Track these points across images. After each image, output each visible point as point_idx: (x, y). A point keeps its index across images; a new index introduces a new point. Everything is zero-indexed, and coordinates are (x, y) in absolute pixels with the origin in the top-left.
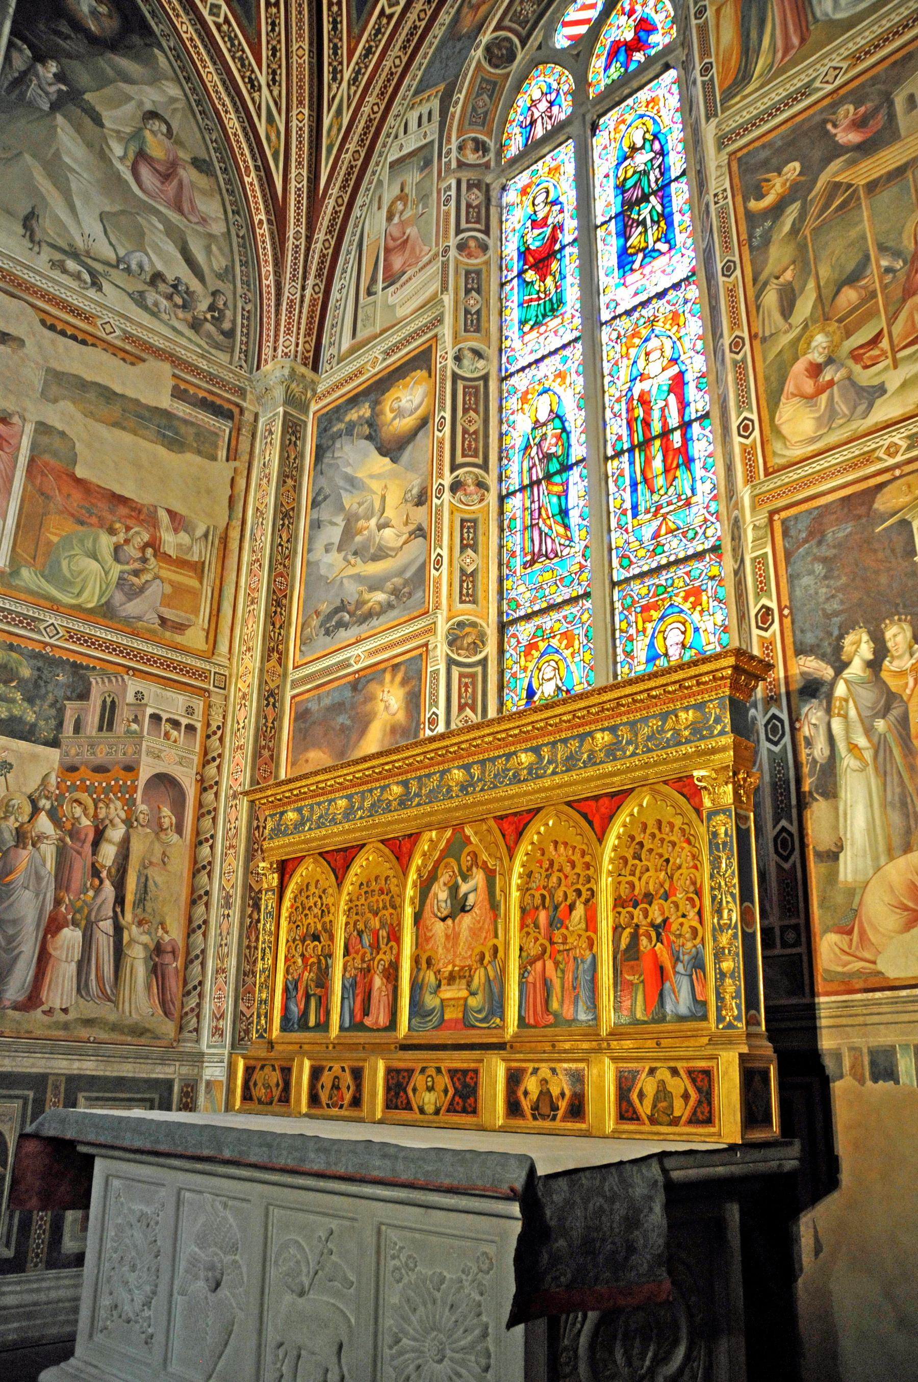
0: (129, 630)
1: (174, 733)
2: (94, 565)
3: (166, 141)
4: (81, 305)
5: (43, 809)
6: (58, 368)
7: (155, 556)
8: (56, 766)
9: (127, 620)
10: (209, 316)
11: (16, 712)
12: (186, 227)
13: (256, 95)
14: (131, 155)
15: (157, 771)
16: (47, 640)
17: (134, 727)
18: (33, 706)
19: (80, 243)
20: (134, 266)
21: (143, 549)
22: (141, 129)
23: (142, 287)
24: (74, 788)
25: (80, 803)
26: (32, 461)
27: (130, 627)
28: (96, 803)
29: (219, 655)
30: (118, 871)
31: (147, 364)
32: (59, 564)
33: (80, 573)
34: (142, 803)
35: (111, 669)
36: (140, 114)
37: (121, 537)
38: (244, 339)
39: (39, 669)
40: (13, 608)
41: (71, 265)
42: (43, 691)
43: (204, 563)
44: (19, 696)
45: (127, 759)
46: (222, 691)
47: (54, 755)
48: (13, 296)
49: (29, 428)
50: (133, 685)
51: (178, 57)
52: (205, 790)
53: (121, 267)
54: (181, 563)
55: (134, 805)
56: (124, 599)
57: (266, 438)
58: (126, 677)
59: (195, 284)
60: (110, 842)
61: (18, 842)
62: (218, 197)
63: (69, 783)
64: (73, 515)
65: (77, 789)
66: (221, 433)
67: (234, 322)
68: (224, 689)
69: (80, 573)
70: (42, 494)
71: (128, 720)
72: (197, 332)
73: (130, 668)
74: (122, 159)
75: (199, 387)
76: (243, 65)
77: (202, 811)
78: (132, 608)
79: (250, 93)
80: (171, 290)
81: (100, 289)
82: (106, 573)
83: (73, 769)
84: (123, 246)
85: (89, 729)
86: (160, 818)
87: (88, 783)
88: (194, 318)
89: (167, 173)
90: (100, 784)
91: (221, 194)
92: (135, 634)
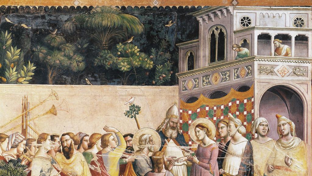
11: (136, 63)
15: (270, 86)
17: (245, 50)
18: (149, 55)
24: (196, 115)
39: (150, 22)
44: (136, 49)
45: (241, 81)
50: (238, 15)
55: (253, 119)
58: (231, 8)
60: (233, 155)
63: (190, 112)
83: (192, 99)
86: (279, 126)
87: (207, 109)
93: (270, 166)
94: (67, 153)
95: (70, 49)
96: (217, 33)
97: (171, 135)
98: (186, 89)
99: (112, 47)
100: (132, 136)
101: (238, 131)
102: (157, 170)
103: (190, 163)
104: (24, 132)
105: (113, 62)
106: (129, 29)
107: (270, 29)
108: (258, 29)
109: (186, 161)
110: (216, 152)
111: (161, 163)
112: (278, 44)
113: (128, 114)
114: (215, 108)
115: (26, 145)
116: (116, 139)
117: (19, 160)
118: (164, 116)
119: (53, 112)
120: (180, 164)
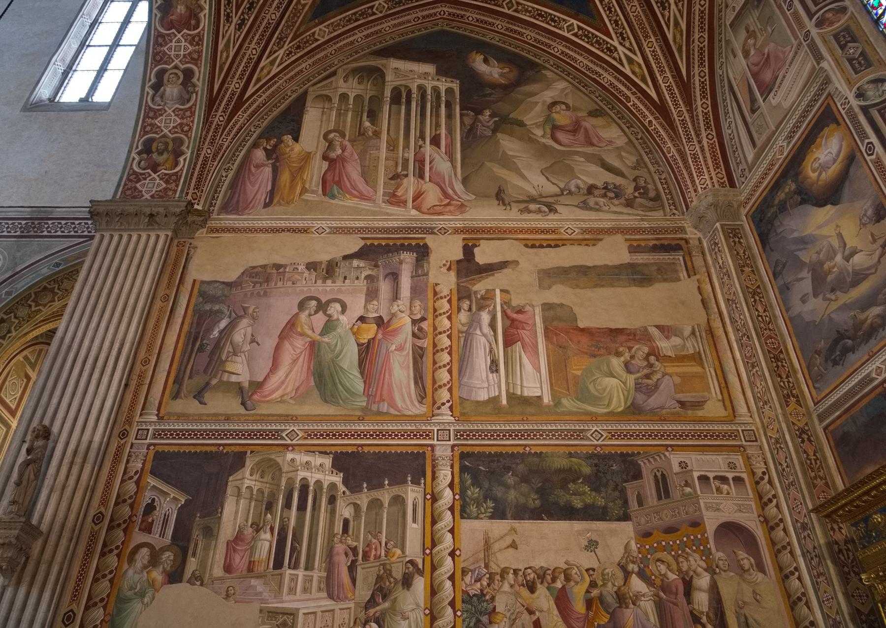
0: (656, 418)
1: (725, 487)
2: (613, 381)
3: (568, 113)
4: (547, 226)
5: (633, 572)
6: (545, 268)
7: (658, 360)
8: (632, 535)
9: (652, 411)
10: (636, 194)
11: (589, 501)
12: (599, 151)
13: (615, 55)
14: (549, 131)
16: (596, 442)
17: (688, 490)
18: (600, 495)
19: (534, 193)
20: (573, 189)
21: (647, 358)
22: (549, 115)
23: (583, 198)
25: (663, 561)
26: (546, 329)
27: (656, 415)
28: (676, 558)
29: (741, 416)
30: (716, 615)
31: (604, 241)
32: (587, 388)
33: (605, 390)
34: (717, 551)
35: (652, 450)
36: (546, 107)
37: (627, 356)
38: (669, 196)
39: (596, 465)
40: (564, 428)
41: (533, 207)
42: (604, 480)
43: (699, 353)
44: (587, 489)
46: (755, 443)
47: (627, 528)
48: (503, 239)
49: (538, 310)
50: (675, 459)
51: (558, 67)
52: (772, 529)
53: (565, 193)
54: (681, 359)
55: (711, 554)
56: (645, 397)
57: (713, 250)
58: (667, 454)
59: (619, 180)
60: (700, 590)
61: (620, 603)
62: (614, 124)
64: (586, 353)
65: (656, 550)
66: (678, 261)
67: (657, 189)
68: (756, 441)
69: (605, 390)
70: (560, 347)
71: (680, 485)
72: (632, 207)
73: (667, 446)
74: (543, 136)
75: (648, 240)
76: (600, 44)
77: (777, 547)
78: (653, 402)
79: (610, 56)
80: (604, 191)
81: (556, 211)
82: (625, 384)
83: (647, 535)
84: (561, 181)
85: (650, 499)
86: (739, 561)
87: (664, 543)
88: (626, 200)
89: (575, 128)
90: (674, 542)
91: (616, 123)
92: (663, 420)
93: (740, 602)
94: (532, 588)
95: (524, 487)
96: (659, 474)
97: (633, 569)
98: (639, 525)
99: (564, 487)
100: (594, 570)
101: (698, 565)
102: (624, 606)
103: (657, 599)
104: (487, 566)
105: (567, 501)
106: (578, 470)
107: (707, 471)
108: (695, 471)
109: (652, 596)
110: (681, 589)
111: (627, 598)
112: (717, 484)
113: (587, 548)
114: (671, 543)
115: (489, 579)
116: (578, 573)
117: (483, 595)
118: (623, 551)
119: (514, 545)
120: (648, 599)
